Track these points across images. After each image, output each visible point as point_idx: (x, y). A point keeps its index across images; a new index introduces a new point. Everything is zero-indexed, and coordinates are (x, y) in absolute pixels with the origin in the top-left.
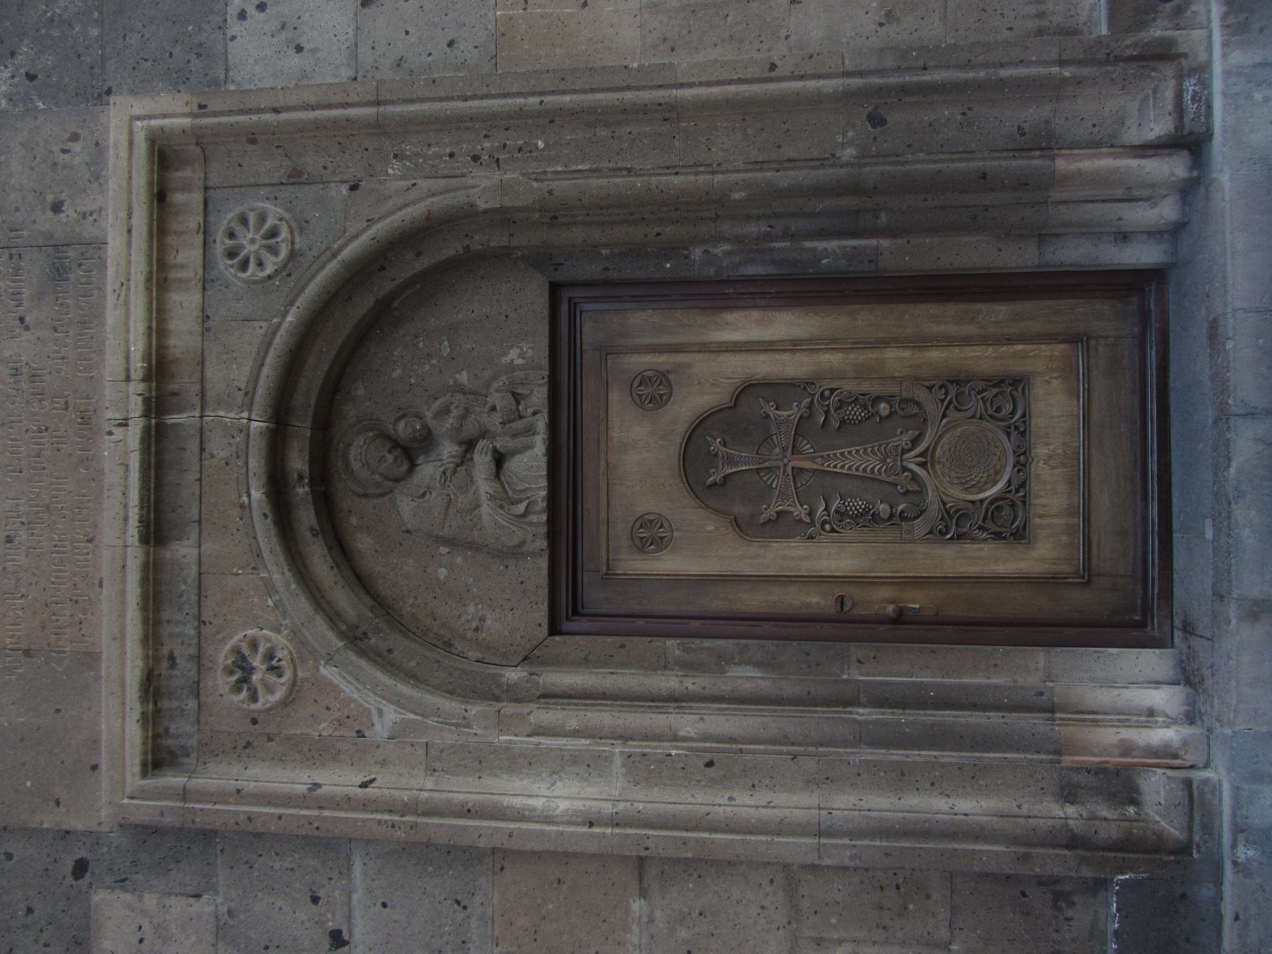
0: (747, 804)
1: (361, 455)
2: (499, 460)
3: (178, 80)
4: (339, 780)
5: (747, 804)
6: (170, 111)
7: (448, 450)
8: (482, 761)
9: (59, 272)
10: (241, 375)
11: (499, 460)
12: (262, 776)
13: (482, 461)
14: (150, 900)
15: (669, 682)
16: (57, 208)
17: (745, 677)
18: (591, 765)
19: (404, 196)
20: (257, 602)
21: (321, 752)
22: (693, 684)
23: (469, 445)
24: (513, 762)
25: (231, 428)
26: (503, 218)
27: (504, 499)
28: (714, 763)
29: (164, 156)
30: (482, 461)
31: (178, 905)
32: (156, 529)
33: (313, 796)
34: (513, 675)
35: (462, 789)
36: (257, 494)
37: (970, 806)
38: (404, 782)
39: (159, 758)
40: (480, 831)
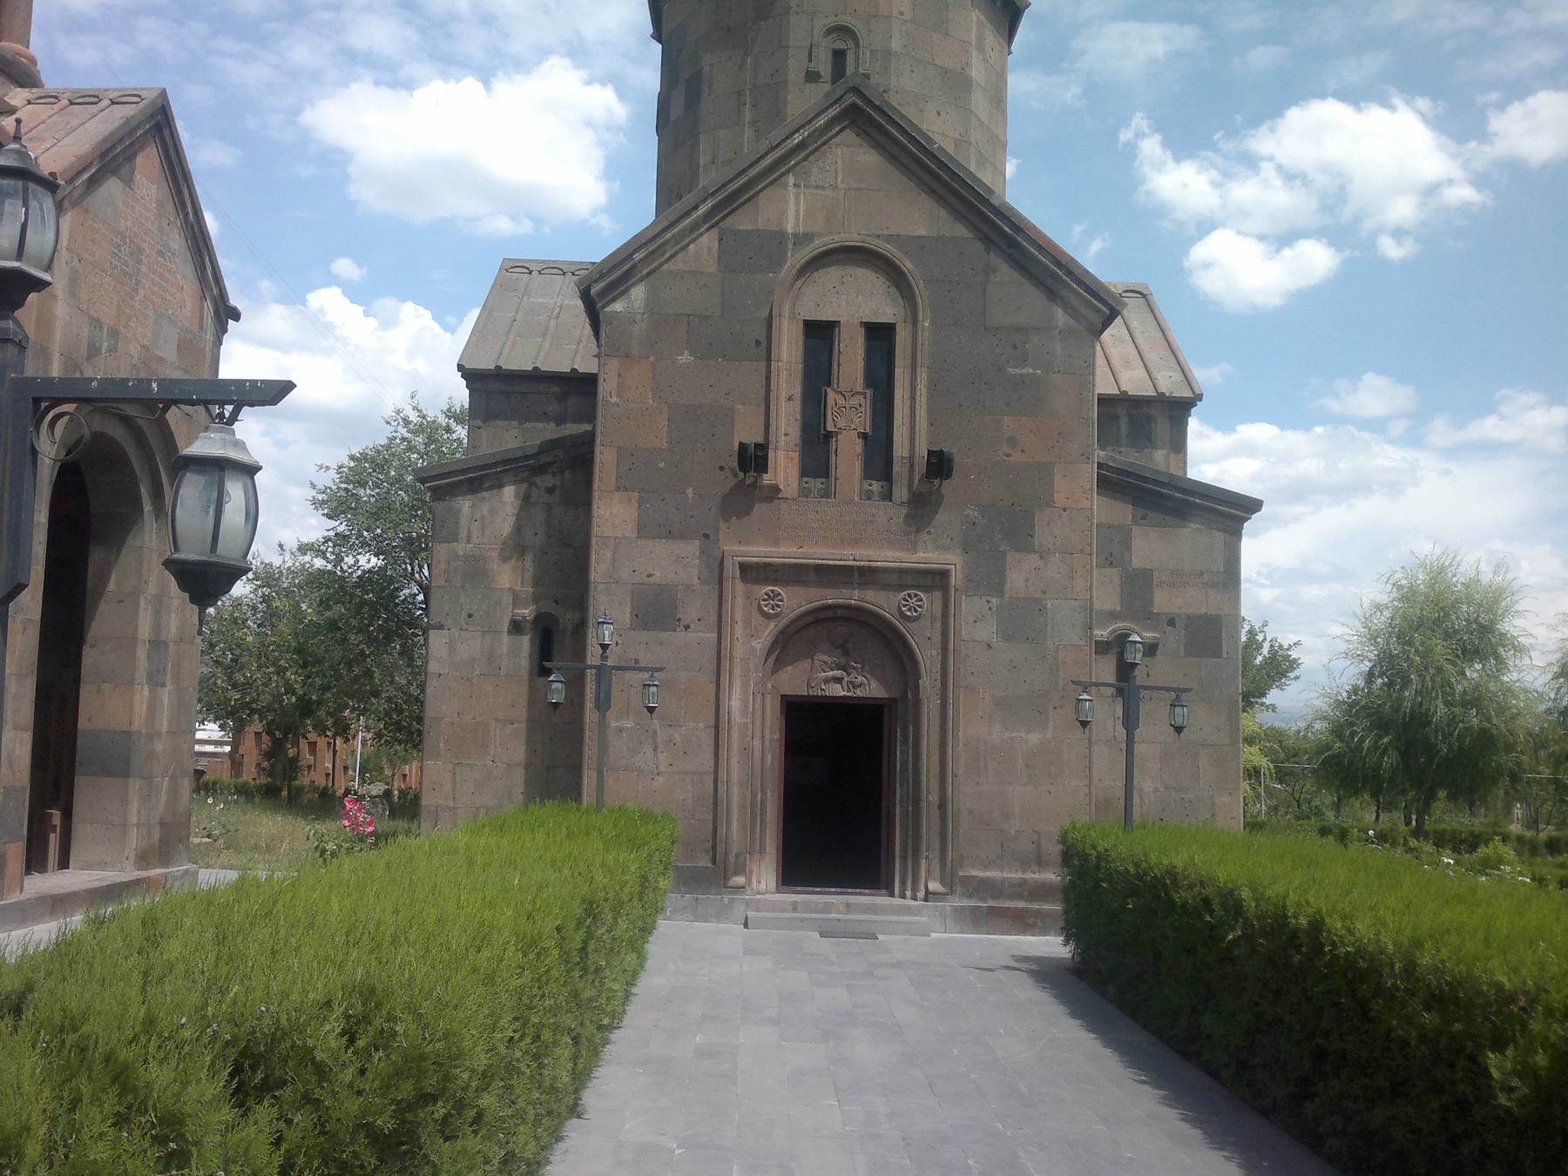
0: (734, 760)
4: (739, 631)
6: (956, 580)
15: (767, 736)
20: (795, 601)
21: (747, 623)
24: (745, 686)
26: (917, 687)
27: (827, 681)
28: (746, 750)
29: (944, 574)
31: (696, 571)
33: (734, 622)
35: (737, 671)
37: (735, 826)
38: (739, 652)
39: (743, 567)
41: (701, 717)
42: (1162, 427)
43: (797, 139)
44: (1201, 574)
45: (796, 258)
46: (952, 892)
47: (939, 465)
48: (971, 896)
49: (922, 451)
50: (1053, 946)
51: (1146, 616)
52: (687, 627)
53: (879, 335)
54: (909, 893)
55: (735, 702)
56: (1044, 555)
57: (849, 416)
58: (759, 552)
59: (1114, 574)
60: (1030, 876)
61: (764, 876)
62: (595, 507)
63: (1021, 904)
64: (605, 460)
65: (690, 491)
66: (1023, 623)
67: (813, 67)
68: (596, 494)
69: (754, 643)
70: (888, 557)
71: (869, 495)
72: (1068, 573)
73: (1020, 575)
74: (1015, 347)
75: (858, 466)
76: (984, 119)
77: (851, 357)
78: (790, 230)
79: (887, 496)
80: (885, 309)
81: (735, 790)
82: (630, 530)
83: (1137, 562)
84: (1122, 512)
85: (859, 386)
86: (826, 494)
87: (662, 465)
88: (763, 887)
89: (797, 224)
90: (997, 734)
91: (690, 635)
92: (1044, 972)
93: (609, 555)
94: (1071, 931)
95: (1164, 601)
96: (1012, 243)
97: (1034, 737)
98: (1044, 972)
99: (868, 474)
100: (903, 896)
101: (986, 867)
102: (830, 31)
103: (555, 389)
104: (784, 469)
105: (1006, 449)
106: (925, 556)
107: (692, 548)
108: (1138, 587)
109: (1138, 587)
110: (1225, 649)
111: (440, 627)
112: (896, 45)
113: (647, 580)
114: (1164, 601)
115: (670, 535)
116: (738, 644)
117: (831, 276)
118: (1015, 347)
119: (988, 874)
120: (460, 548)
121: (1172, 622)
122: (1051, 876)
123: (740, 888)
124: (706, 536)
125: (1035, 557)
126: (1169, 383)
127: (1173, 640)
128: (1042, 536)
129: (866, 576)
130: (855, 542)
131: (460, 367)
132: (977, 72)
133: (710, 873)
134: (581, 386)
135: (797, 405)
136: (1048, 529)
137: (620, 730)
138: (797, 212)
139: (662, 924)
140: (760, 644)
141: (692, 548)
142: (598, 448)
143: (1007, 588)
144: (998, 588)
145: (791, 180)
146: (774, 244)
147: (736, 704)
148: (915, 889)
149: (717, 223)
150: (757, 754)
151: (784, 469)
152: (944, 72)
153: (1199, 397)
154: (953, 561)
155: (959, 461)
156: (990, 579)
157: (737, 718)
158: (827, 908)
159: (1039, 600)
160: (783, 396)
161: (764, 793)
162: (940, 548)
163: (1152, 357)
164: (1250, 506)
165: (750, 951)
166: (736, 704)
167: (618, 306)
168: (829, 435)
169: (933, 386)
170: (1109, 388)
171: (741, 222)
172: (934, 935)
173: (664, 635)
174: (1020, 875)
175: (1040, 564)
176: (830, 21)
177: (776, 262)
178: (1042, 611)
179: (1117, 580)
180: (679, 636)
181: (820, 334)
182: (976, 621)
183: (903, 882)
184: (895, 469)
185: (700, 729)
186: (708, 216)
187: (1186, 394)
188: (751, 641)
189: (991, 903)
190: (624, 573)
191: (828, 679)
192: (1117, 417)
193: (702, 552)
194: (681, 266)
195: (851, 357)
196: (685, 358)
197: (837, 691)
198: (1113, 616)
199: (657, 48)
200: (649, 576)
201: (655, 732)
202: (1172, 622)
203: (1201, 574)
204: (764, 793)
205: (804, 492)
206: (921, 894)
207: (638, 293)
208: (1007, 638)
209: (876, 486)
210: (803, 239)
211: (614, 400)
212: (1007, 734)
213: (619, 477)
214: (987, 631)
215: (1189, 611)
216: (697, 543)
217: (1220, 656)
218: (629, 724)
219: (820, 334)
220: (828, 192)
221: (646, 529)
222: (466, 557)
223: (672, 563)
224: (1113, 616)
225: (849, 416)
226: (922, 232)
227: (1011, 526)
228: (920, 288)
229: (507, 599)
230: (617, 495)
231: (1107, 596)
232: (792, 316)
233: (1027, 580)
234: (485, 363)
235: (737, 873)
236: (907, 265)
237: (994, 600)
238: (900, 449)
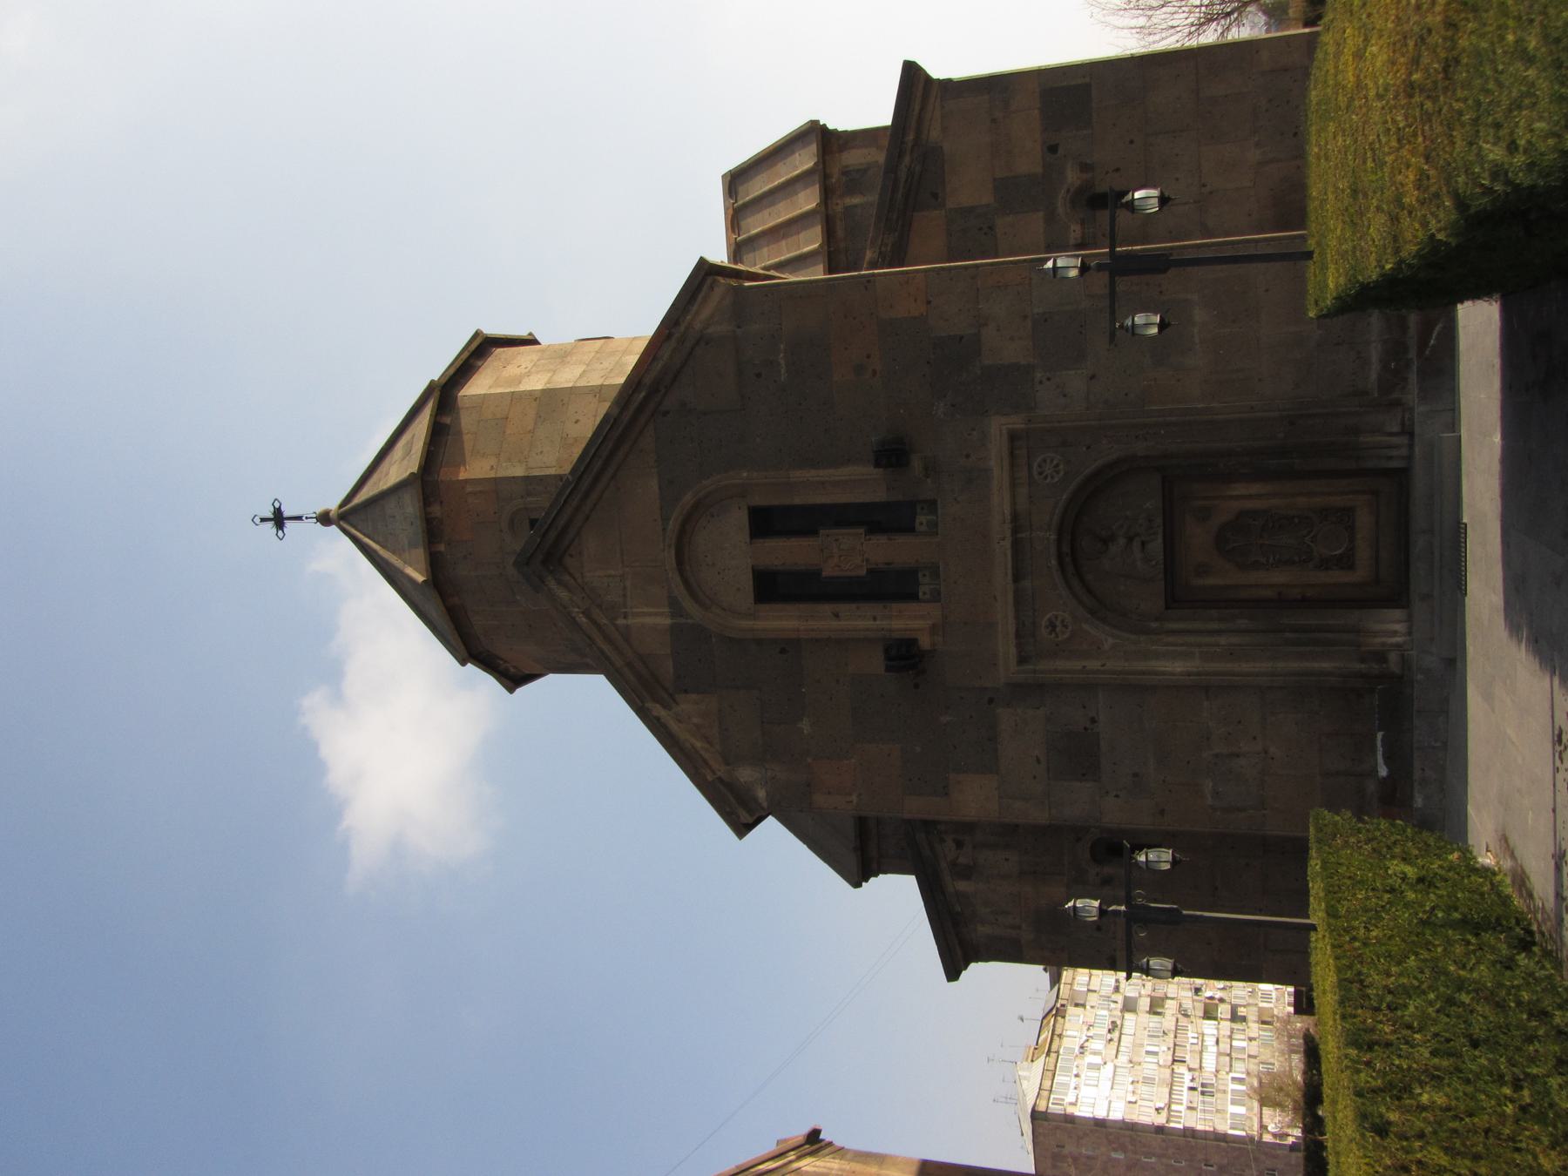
0: (1245, 667)
2: (1143, 544)
4: (1093, 664)
5: (1245, 667)
6: (1017, 422)
7: (1122, 541)
12: (1061, 664)
13: (1136, 544)
15: (1215, 626)
16: (968, 456)
17: (1243, 623)
23: (1130, 540)
29: (1013, 437)
32: (1017, 578)
34: (1154, 625)
35: (1141, 666)
36: (1054, 562)
37: (1326, 665)
39: (1022, 660)
42: (853, 158)
43: (583, 620)
44: (994, 121)
47: (892, 455)
49: (876, 473)
52: (1093, 721)
53: (764, 523)
57: (847, 554)
64: (916, 807)
69: (1106, 647)
70: (1000, 502)
74: (759, 375)
75: (901, 539)
76: (579, 370)
77: (786, 553)
78: (668, 621)
79: (932, 505)
80: (738, 519)
81: (1281, 665)
87: (918, 749)
89: (661, 614)
95: (1028, 162)
97: (1199, 315)
108: (1013, 193)
110: (1080, 81)
114: (1028, 162)
118: (759, 375)
121: (1053, 149)
124: (991, 701)
135: (844, 608)
138: (650, 614)
145: (620, 622)
147: (1178, 667)
149: (671, 696)
150: (1235, 640)
154: (998, 427)
157: (1193, 665)
160: (834, 624)
164: (911, 72)
166: (1178, 667)
168: (870, 571)
181: (770, 587)
186: (666, 707)
195: (786, 553)
196: (805, 726)
200: (1038, 761)
201: (1217, 756)
202: (1053, 149)
203: (994, 121)
205: (936, 597)
207: (745, 774)
209: (922, 520)
210: (676, 608)
211: (854, 798)
219: (770, 587)
225: (847, 554)
226: (654, 484)
233: (1012, 339)
236: (688, 499)
238: (879, 495)
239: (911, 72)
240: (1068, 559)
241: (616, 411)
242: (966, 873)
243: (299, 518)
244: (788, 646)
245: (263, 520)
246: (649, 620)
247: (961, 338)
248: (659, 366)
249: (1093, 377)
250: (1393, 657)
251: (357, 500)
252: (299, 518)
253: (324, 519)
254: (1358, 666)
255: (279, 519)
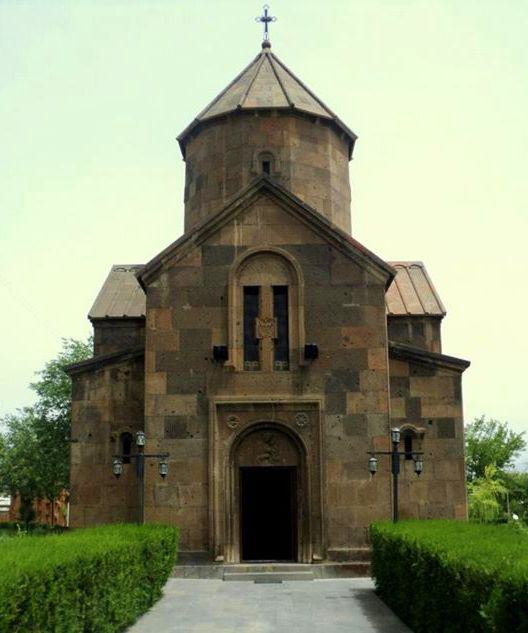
0: (217, 500)
1: (268, 434)
2: (268, 458)
3: (328, 406)
6: (322, 406)
7: (269, 449)
8: (221, 458)
9: (297, 385)
10: (281, 418)
11: (268, 458)
13: (267, 455)
14: (196, 404)
17: (234, 498)
18: (221, 477)
19: (307, 443)
20: (243, 422)
21: (221, 433)
22: (233, 490)
23: (269, 453)
24: (221, 464)
25: (272, 417)
26: (305, 460)
27: (261, 459)
28: (222, 495)
29: (316, 405)
30: (267, 455)
31: (194, 409)
32: (255, 405)
33: (214, 432)
35: (217, 456)
36: (261, 421)
38: (217, 448)
39: (218, 406)
40: (211, 460)
41: (201, 477)
42: (429, 330)
43: (238, 204)
45: (238, 259)
46: (325, 557)
47: (311, 353)
48: (334, 560)
49: (303, 345)
50: (368, 583)
51: (419, 421)
53: (280, 292)
54: (305, 560)
55: (216, 472)
56: (364, 393)
57: (266, 332)
58: (224, 398)
59: (402, 400)
60: (362, 549)
61: (233, 557)
62: (146, 378)
63: (358, 563)
64: (150, 357)
65: (191, 371)
66: (356, 426)
67: (253, 170)
68: (146, 374)
70: (285, 397)
71: (278, 369)
72: (377, 404)
73: (353, 403)
75: (272, 354)
77: (267, 302)
78: (236, 244)
79: (287, 368)
80: (281, 281)
81: (217, 514)
82: (163, 392)
83: (413, 393)
84: (404, 370)
85: (272, 317)
86: (258, 368)
88: (233, 561)
90: (345, 481)
91: (193, 439)
92: (362, 597)
93: (153, 403)
94: (375, 573)
95: (427, 412)
96: (342, 246)
97: (363, 482)
98: (362, 597)
99: (277, 357)
100: (302, 562)
101: (341, 545)
102: (261, 154)
103: (134, 325)
104: (236, 358)
105: (344, 342)
106: (308, 397)
107: (193, 398)
108: (414, 407)
109: (414, 407)
111: (76, 441)
112: (293, 158)
113: (171, 414)
114: (427, 412)
115: (183, 392)
116: (217, 444)
117: (257, 264)
118: (346, 294)
119: (344, 549)
120: (85, 403)
121: (431, 422)
122: (367, 549)
123: (221, 562)
124: (200, 392)
125: (360, 395)
126: (431, 309)
127: (432, 430)
128: (363, 384)
129: (278, 406)
130: (273, 391)
131: (89, 317)
132: (333, 168)
133: (202, 555)
134: (140, 321)
136: (367, 380)
137: (161, 488)
139: (169, 579)
140: (228, 442)
141: (193, 398)
142: (146, 352)
143: (348, 410)
144: (343, 411)
145: (235, 222)
146: (230, 251)
147: (216, 472)
148: (307, 558)
150: (228, 496)
151: (236, 358)
152: (317, 169)
153: (445, 314)
155: (320, 348)
156: (338, 405)
158: (264, 569)
159: (363, 415)
160: (235, 323)
161: (232, 516)
162: (313, 392)
163: (423, 297)
164: (466, 364)
165: (221, 591)
166: (216, 472)
167: (155, 285)
168: (258, 340)
169: (307, 314)
170: (401, 311)
171: (209, 243)
172: (315, 580)
173: (181, 441)
174: (358, 549)
175: (363, 397)
176: (261, 150)
177: (229, 259)
178: (364, 419)
179: (404, 403)
180: (188, 441)
181: (251, 293)
182: (333, 427)
183: (302, 556)
184: (291, 355)
185: (198, 485)
186: (197, 241)
187: (439, 312)
188: (221, 443)
189: (344, 563)
190: (161, 411)
191: (264, 457)
192: (407, 325)
193: (199, 400)
194: (184, 264)
195: (267, 302)
197: (267, 464)
198: (403, 421)
199: (184, 163)
202: (431, 422)
204: (232, 516)
205: (247, 369)
206: (310, 561)
207: (164, 277)
208: (348, 434)
209: (281, 364)
210: (243, 248)
211: (154, 328)
212: (350, 482)
213: (156, 366)
214: (338, 431)
215: (440, 416)
216: (196, 395)
217: (454, 437)
218: (165, 484)
219: (251, 293)
220: (253, 227)
221: (171, 389)
222: (88, 408)
223: (183, 406)
224: (403, 421)
225: (266, 332)
226: (299, 242)
227: (348, 380)
228: (299, 268)
229: (108, 427)
230: (156, 374)
231: (399, 412)
232: (238, 285)
233: (357, 405)
234: (101, 314)
235: (220, 554)
236: (292, 258)
237: (341, 416)
239: (466, 364)
240: (262, 426)
241: (332, 227)
242: (114, 377)
243: (266, 30)
244: (224, 300)
245: (266, 11)
246: (236, 235)
247: (358, 384)
248: (352, 248)
249: (339, 439)
250: (221, 558)
251: (276, 64)
252: (266, 30)
253: (266, 45)
254: (218, 543)
255: (266, 20)
